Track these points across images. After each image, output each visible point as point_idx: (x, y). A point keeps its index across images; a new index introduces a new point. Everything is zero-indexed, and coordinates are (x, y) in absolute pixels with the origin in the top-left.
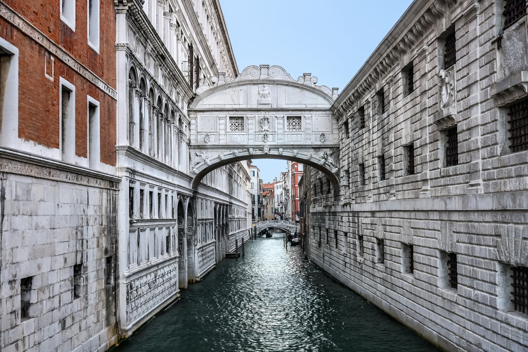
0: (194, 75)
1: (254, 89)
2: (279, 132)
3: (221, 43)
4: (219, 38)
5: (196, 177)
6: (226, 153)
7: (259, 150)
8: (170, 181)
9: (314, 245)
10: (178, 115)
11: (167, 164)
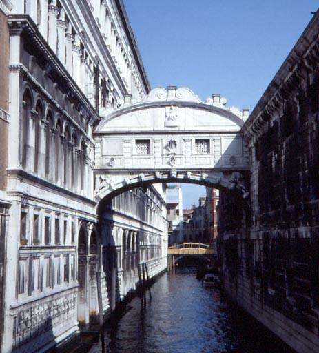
1: (161, 111)
3: (132, 65)
4: (130, 60)
5: (100, 202)
10: (81, 137)
11: (67, 189)
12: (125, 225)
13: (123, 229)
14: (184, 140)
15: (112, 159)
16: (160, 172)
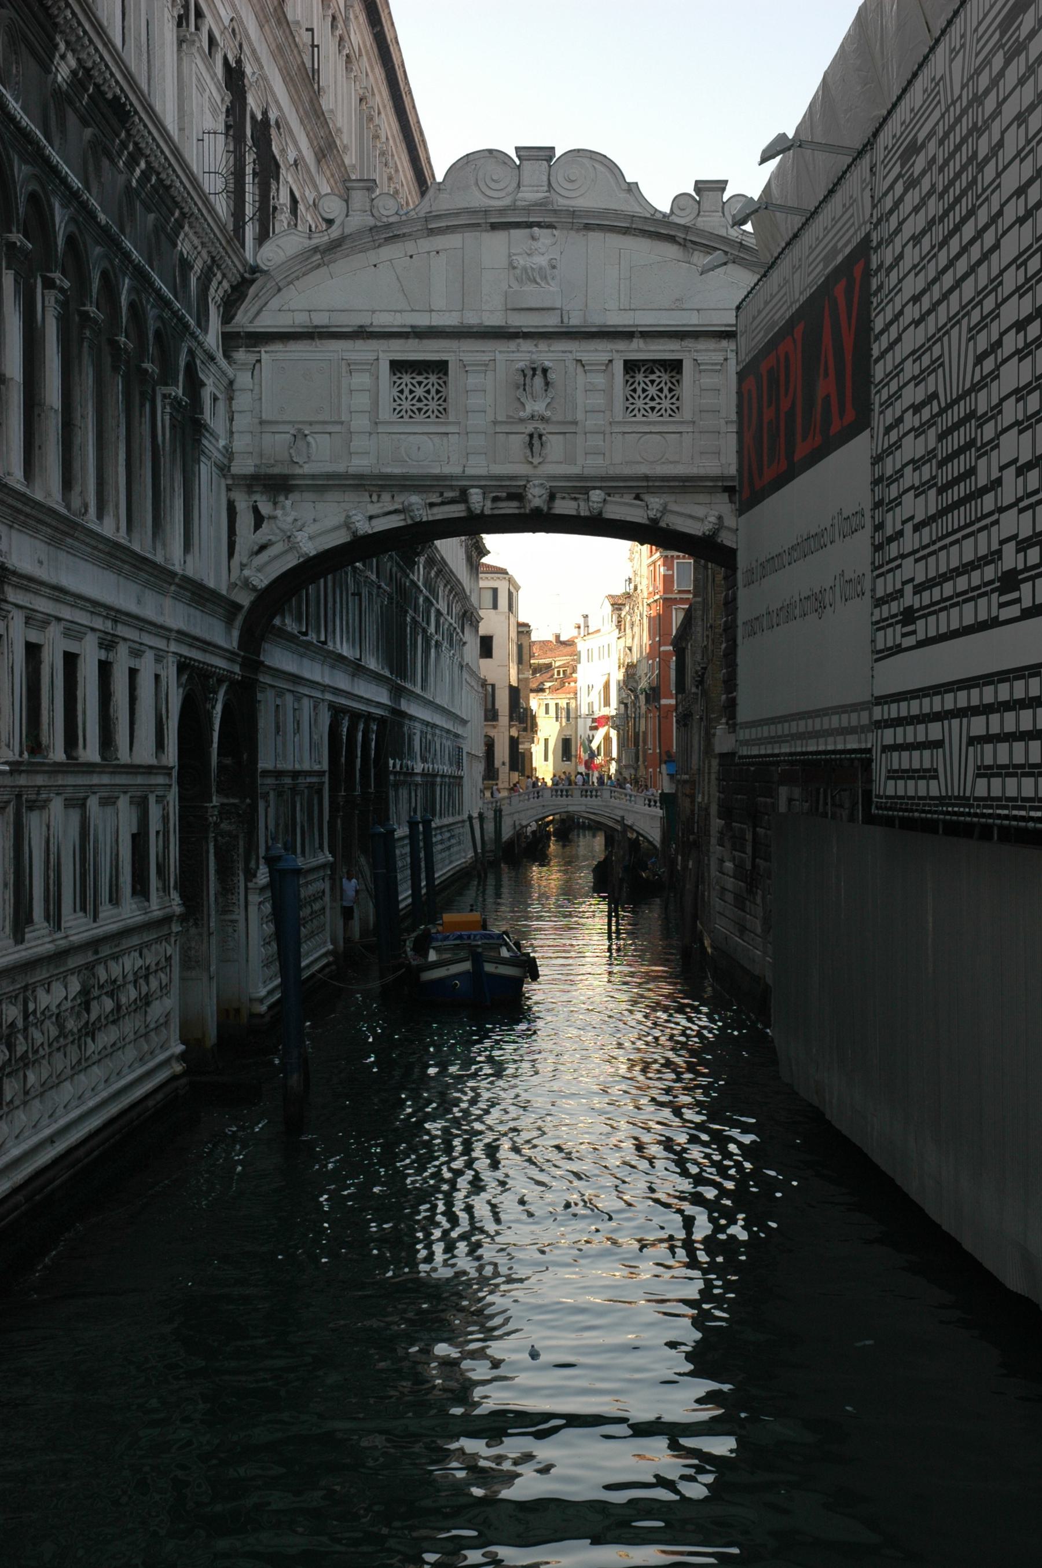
0: (249, 188)
2: (591, 423)
3: (365, 58)
5: (253, 604)
6: (374, 509)
7: (511, 497)
8: (149, 612)
9: (730, 883)
12: (337, 691)
13: (334, 708)
14: (577, 361)
15: (299, 436)
16: (484, 493)
